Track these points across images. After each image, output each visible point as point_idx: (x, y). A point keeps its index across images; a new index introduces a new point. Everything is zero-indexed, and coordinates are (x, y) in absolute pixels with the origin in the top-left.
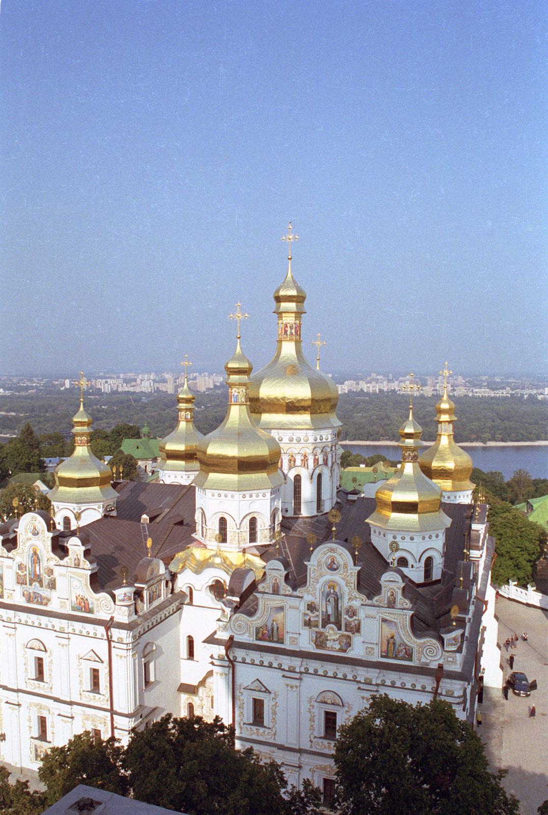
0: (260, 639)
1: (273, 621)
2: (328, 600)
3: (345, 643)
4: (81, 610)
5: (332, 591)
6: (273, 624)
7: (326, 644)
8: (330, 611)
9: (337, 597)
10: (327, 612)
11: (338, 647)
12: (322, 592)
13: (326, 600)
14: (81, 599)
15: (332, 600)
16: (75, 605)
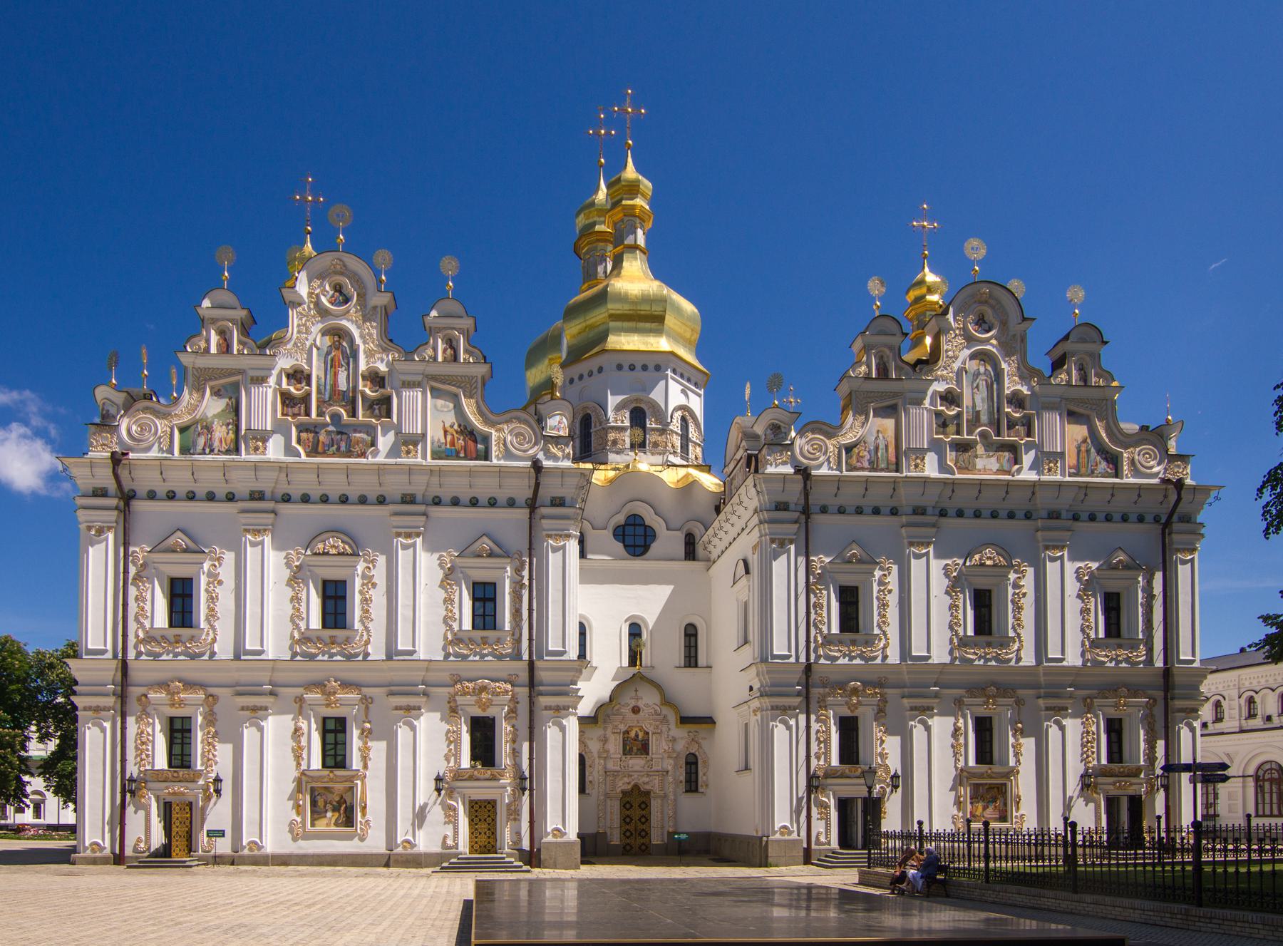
0: (855, 469)
1: (878, 431)
2: (975, 385)
3: (1007, 458)
4: (458, 457)
5: (982, 369)
6: (876, 438)
7: (974, 465)
8: (981, 406)
9: (991, 378)
10: (974, 406)
11: (995, 467)
12: (966, 372)
13: (972, 385)
14: (457, 432)
15: (983, 385)
16: (440, 447)
